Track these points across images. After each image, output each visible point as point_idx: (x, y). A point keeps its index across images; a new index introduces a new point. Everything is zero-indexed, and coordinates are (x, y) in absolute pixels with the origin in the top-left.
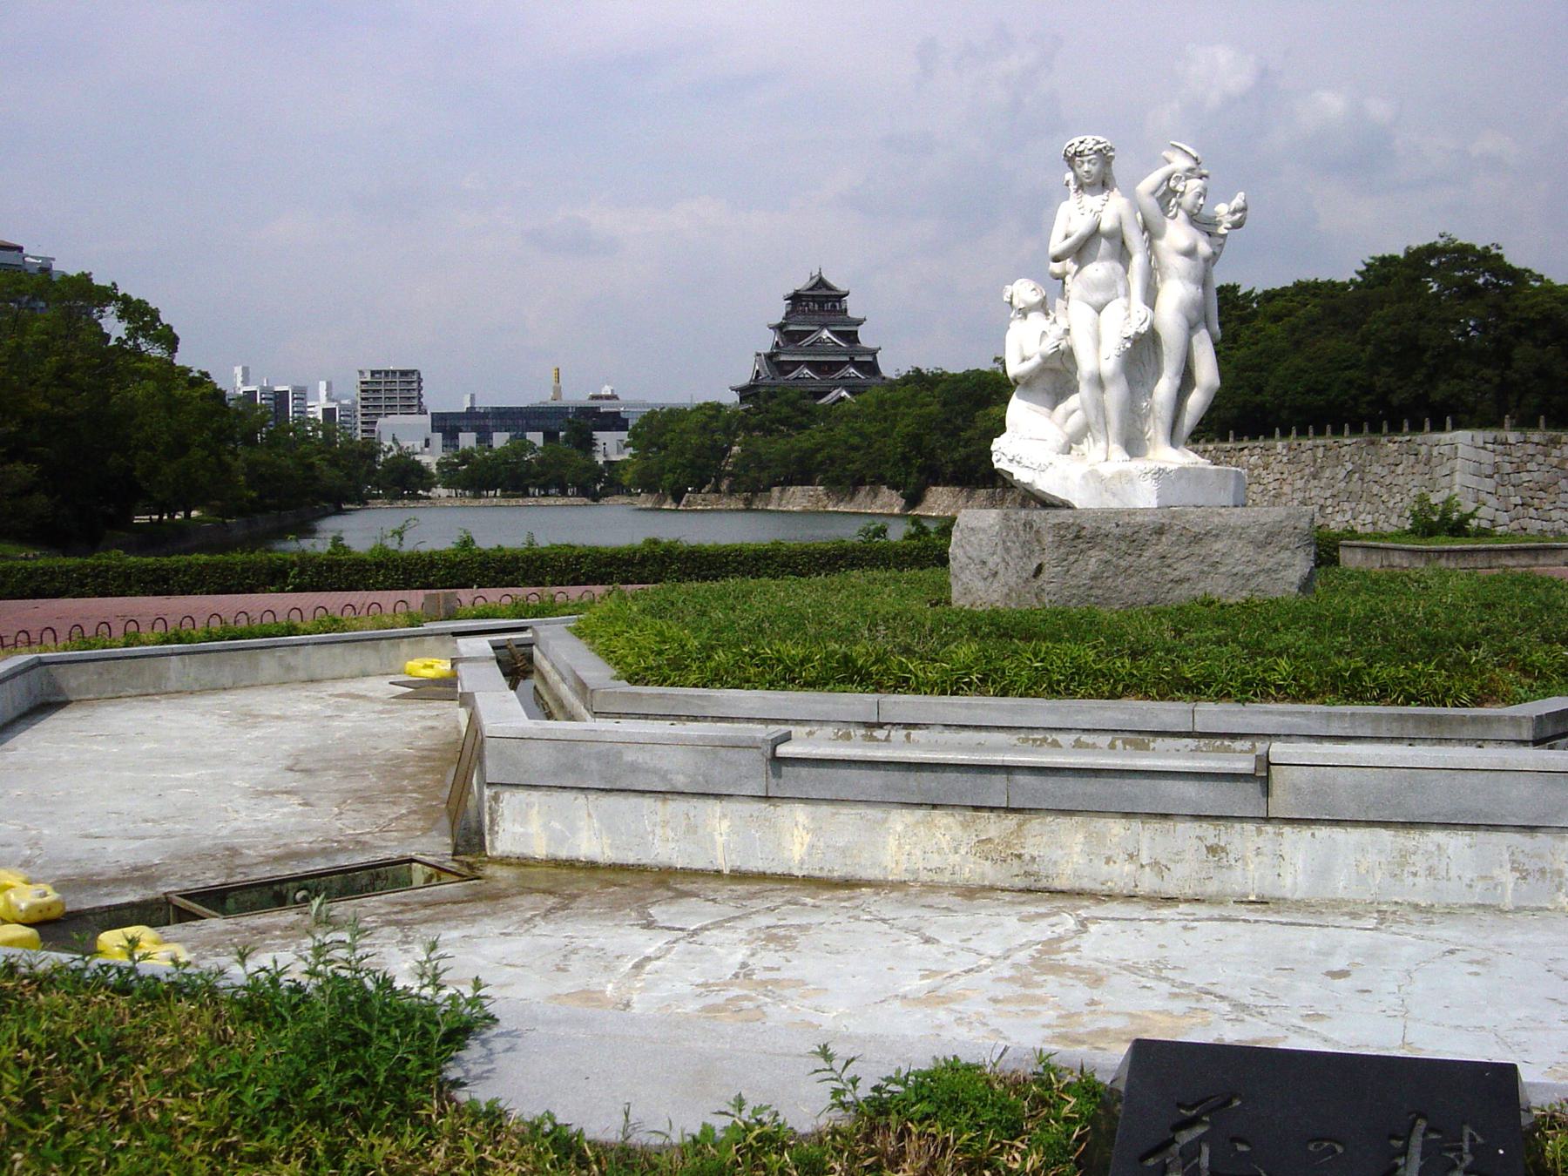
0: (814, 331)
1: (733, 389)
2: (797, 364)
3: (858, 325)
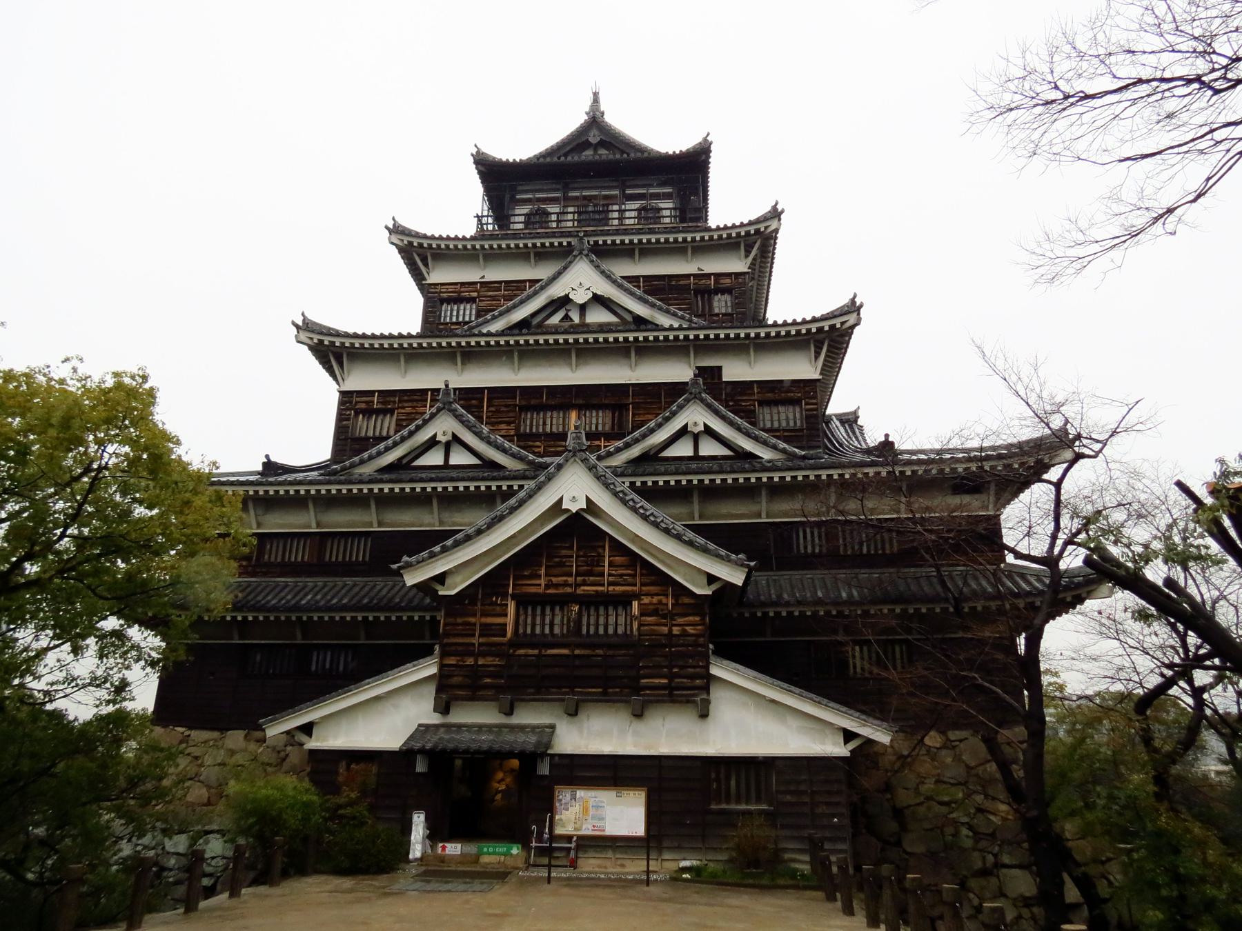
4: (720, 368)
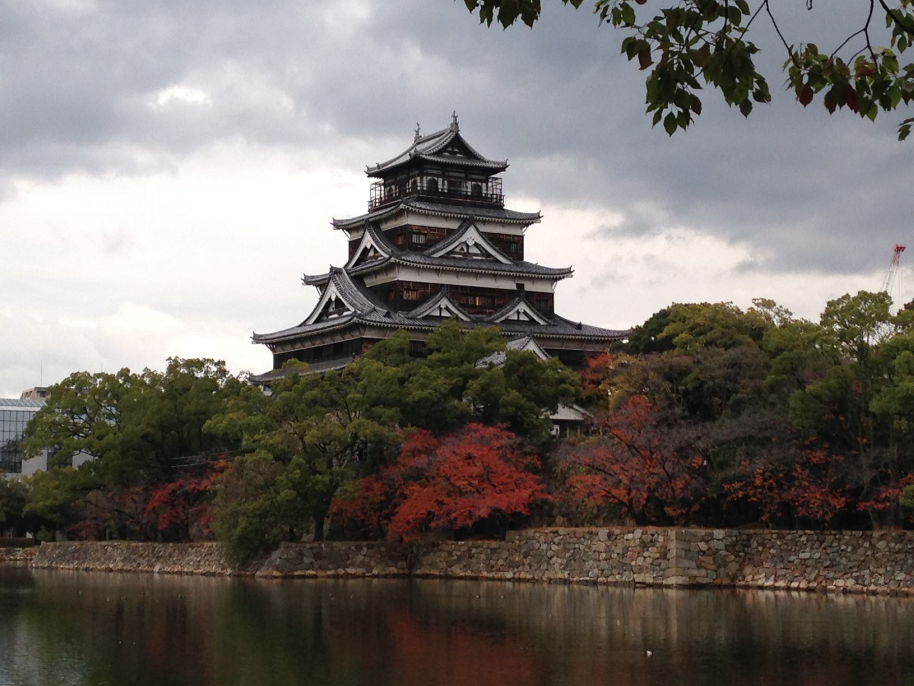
0: (451, 232)
1: (258, 339)
2: (429, 292)
3: (527, 225)
4: (523, 285)
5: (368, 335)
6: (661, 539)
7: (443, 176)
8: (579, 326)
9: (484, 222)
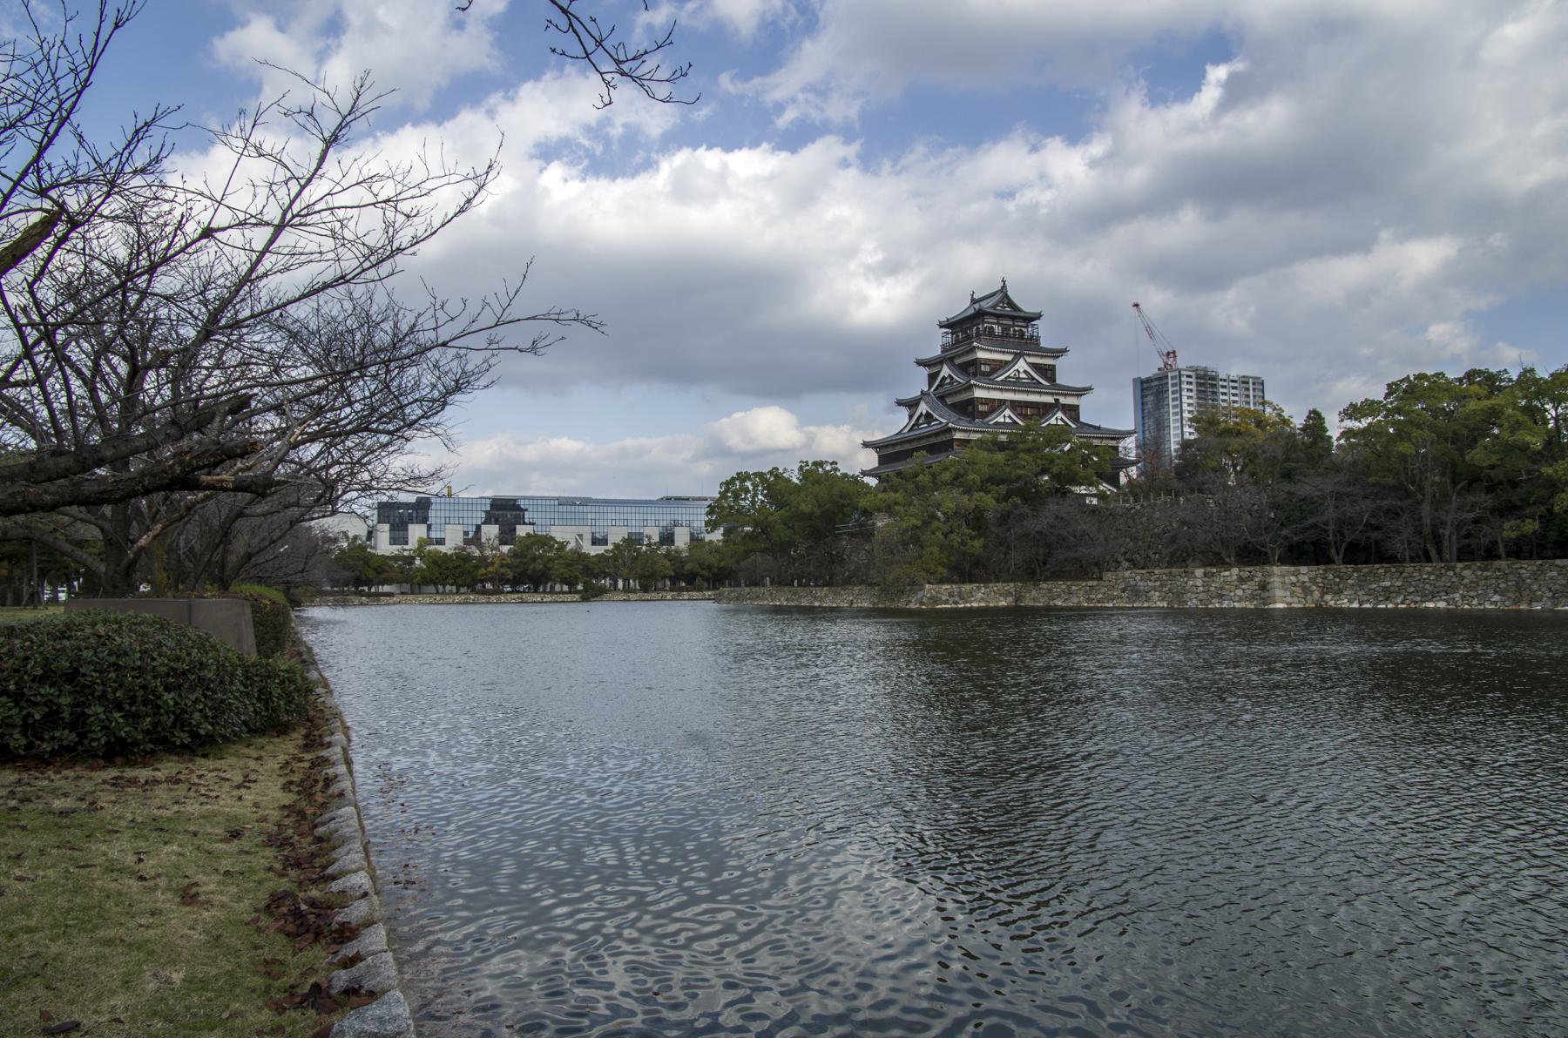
0: (1007, 362)
5: (958, 436)
6: (1259, 574)
7: (997, 324)
8: (1099, 428)
9: (1029, 355)
